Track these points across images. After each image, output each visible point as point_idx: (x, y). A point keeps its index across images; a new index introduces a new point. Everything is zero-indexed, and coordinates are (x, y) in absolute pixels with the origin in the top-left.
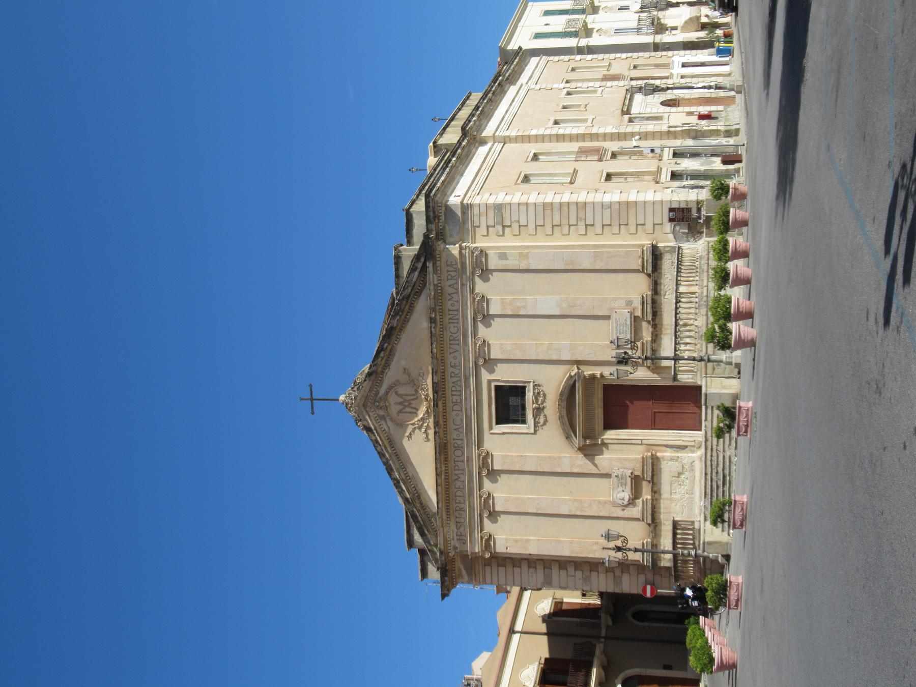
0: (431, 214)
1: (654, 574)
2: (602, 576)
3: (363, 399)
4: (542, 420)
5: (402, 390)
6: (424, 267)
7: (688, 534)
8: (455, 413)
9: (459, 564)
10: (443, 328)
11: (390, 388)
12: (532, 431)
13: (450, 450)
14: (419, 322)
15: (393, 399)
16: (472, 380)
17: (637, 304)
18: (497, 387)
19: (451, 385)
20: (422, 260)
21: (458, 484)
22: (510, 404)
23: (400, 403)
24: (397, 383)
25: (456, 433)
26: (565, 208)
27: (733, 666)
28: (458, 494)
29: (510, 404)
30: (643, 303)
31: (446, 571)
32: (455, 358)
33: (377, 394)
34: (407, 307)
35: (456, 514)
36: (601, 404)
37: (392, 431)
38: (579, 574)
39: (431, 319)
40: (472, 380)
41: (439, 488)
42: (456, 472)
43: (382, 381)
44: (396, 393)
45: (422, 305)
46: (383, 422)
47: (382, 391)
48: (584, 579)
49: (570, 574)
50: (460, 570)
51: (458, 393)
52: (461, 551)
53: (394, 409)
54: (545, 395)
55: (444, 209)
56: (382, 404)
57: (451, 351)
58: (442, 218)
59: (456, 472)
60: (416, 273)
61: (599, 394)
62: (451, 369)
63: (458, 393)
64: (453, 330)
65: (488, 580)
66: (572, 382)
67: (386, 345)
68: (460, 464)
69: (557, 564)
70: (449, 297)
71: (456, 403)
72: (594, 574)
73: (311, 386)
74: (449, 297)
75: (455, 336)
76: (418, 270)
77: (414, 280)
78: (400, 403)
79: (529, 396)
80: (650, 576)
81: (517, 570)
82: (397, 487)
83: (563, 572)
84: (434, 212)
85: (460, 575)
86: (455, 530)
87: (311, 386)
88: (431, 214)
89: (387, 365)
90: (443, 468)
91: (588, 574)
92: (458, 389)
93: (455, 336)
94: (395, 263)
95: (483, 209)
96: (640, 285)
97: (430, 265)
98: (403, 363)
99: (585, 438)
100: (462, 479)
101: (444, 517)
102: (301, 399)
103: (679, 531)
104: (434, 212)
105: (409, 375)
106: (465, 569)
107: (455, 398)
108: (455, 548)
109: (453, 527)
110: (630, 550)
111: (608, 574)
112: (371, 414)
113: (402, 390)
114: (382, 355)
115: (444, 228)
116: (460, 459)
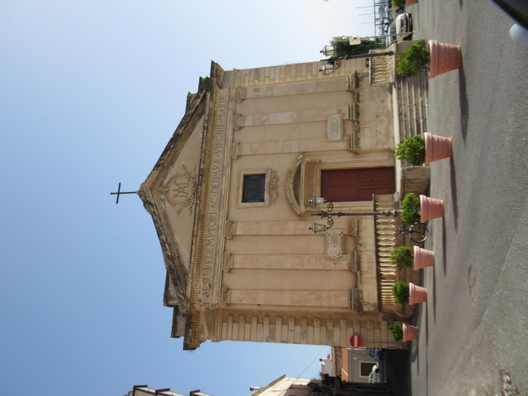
0: (215, 73)
1: (360, 328)
2: (317, 330)
3: (151, 183)
4: (274, 197)
5: (178, 181)
6: (205, 95)
7: (390, 292)
8: (213, 194)
9: (203, 322)
10: (212, 136)
11: (172, 179)
12: (268, 205)
13: (207, 221)
14: (197, 134)
15: (172, 187)
16: (228, 171)
17: (346, 110)
18: (246, 177)
19: (213, 174)
20: (204, 92)
21: (209, 247)
22: (254, 188)
23: (177, 190)
24: (177, 175)
25: (213, 208)
26: (299, 66)
27: (454, 60)
28: (208, 255)
29: (254, 188)
30: (349, 110)
31: (191, 323)
32: (218, 156)
33: (161, 184)
34: (190, 123)
35: (205, 272)
36: (319, 182)
37: (167, 210)
38: (298, 329)
39: (204, 127)
40: (228, 171)
41: (194, 247)
42: (209, 238)
43: (166, 174)
44: (175, 183)
45: (200, 124)
46: (162, 203)
47: (166, 182)
48: (302, 333)
49: (290, 329)
50: (202, 326)
51: (217, 180)
52: (205, 304)
53: (172, 194)
54: (278, 179)
55: (223, 74)
56: (164, 190)
57: (217, 151)
58: (222, 78)
59: (209, 238)
60: (199, 100)
61: (318, 176)
62: (214, 164)
63: (217, 180)
64: (219, 138)
65: (224, 336)
66: (298, 165)
67: (173, 146)
68: (212, 232)
69: (280, 320)
70: (219, 118)
71: (215, 187)
72: (310, 328)
73: (120, 184)
74: (219, 118)
75: (220, 142)
76: (201, 98)
77: (197, 104)
78: (177, 190)
79: (267, 180)
80: (357, 329)
81: (248, 326)
82: (162, 246)
83: (285, 327)
84: (216, 73)
85: (202, 331)
86: (202, 286)
87: (120, 184)
88: (215, 73)
89: (172, 163)
90: (199, 233)
91: (305, 328)
92: (218, 177)
93: (220, 142)
94: (187, 100)
95: (248, 72)
96: (347, 100)
97: (209, 94)
98: (183, 162)
99: (306, 206)
100: (212, 244)
101: (195, 271)
102: (112, 194)
103: (382, 265)
104: (216, 73)
105: (185, 169)
106: (207, 325)
107: (215, 183)
108: (200, 301)
109: (201, 283)
110: (335, 214)
111: (322, 328)
112: (155, 196)
113: (178, 181)
114: (168, 153)
115: (222, 84)
116: (213, 228)
